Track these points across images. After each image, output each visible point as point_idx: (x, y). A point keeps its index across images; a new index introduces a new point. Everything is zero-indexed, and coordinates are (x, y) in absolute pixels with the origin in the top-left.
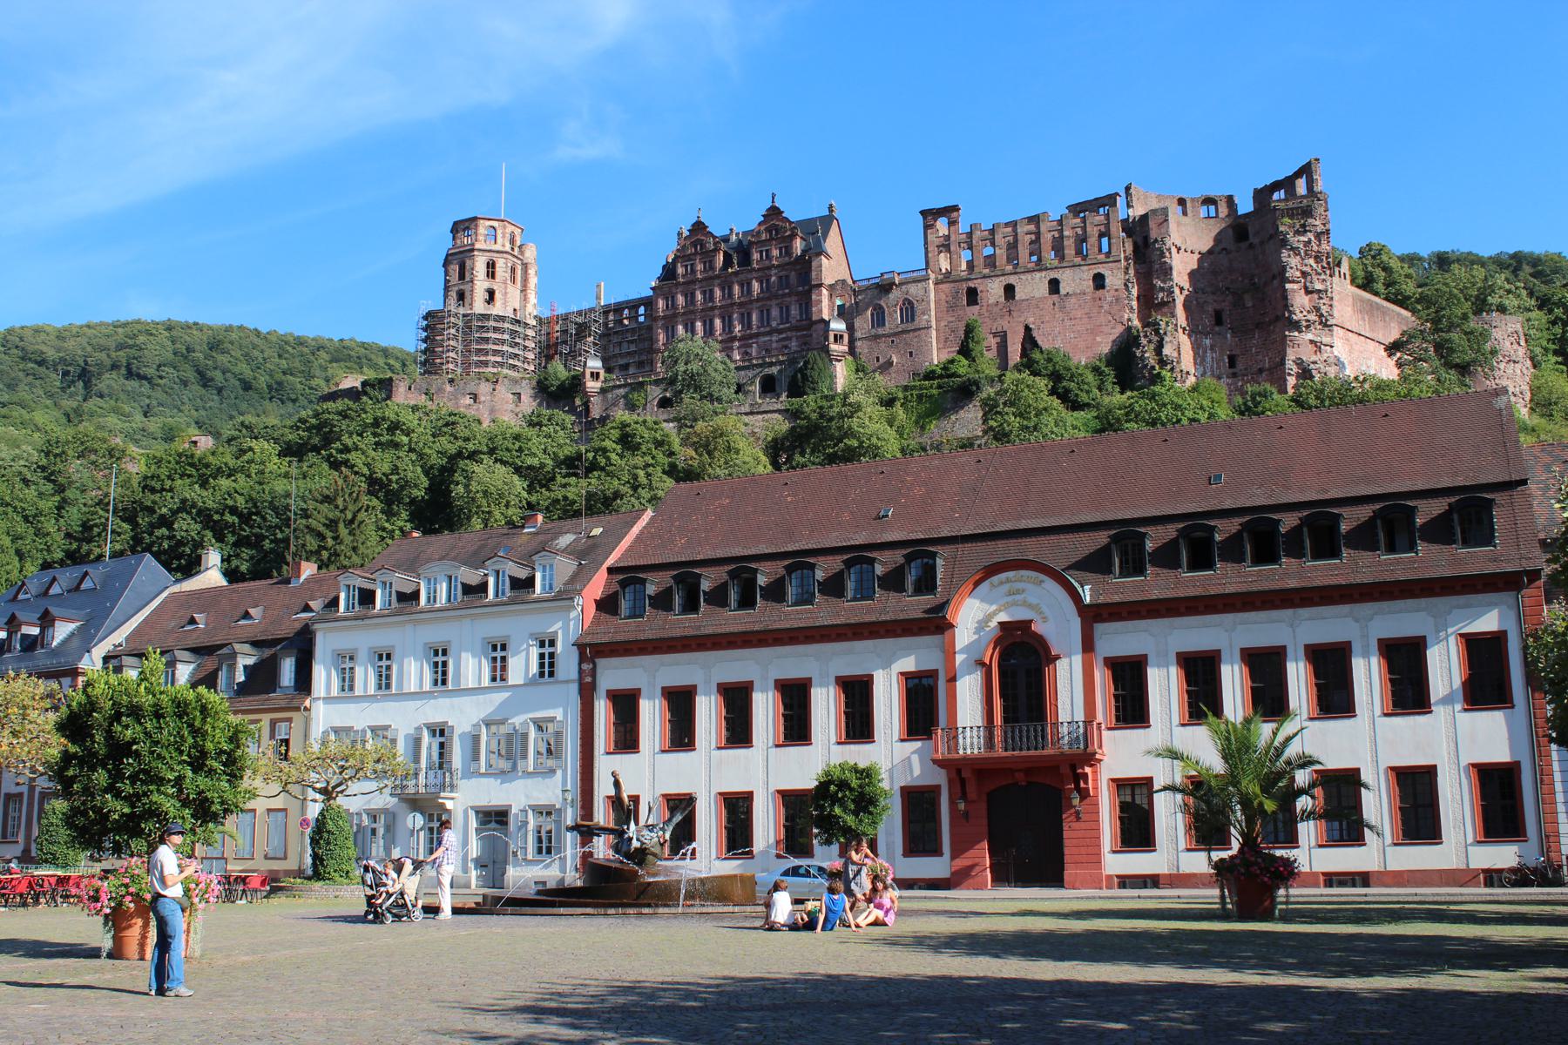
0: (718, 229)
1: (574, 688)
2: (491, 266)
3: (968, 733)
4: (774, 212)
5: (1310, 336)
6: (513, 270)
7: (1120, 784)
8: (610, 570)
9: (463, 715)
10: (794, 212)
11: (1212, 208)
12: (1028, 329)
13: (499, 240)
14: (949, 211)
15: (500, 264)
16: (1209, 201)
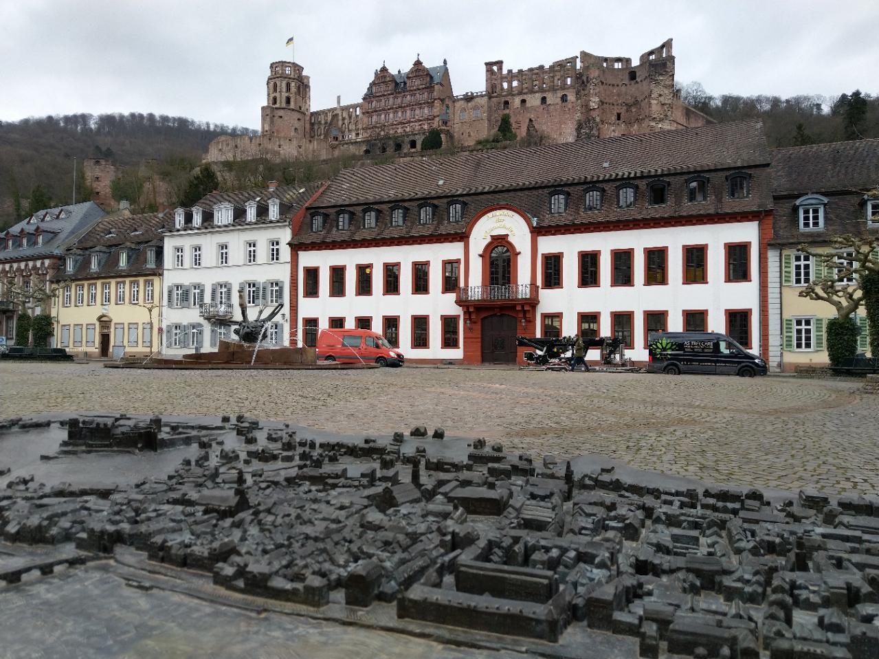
0: (393, 71)
1: (289, 266)
2: (288, 85)
3: (476, 290)
4: (418, 63)
5: (660, 126)
6: (299, 87)
7: (545, 316)
8: (307, 209)
9: (236, 277)
10: (428, 64)
11: (620, 64)
12: (531, 120)
14: (499, 63)
15: (293, 84)
16: (619, 60)
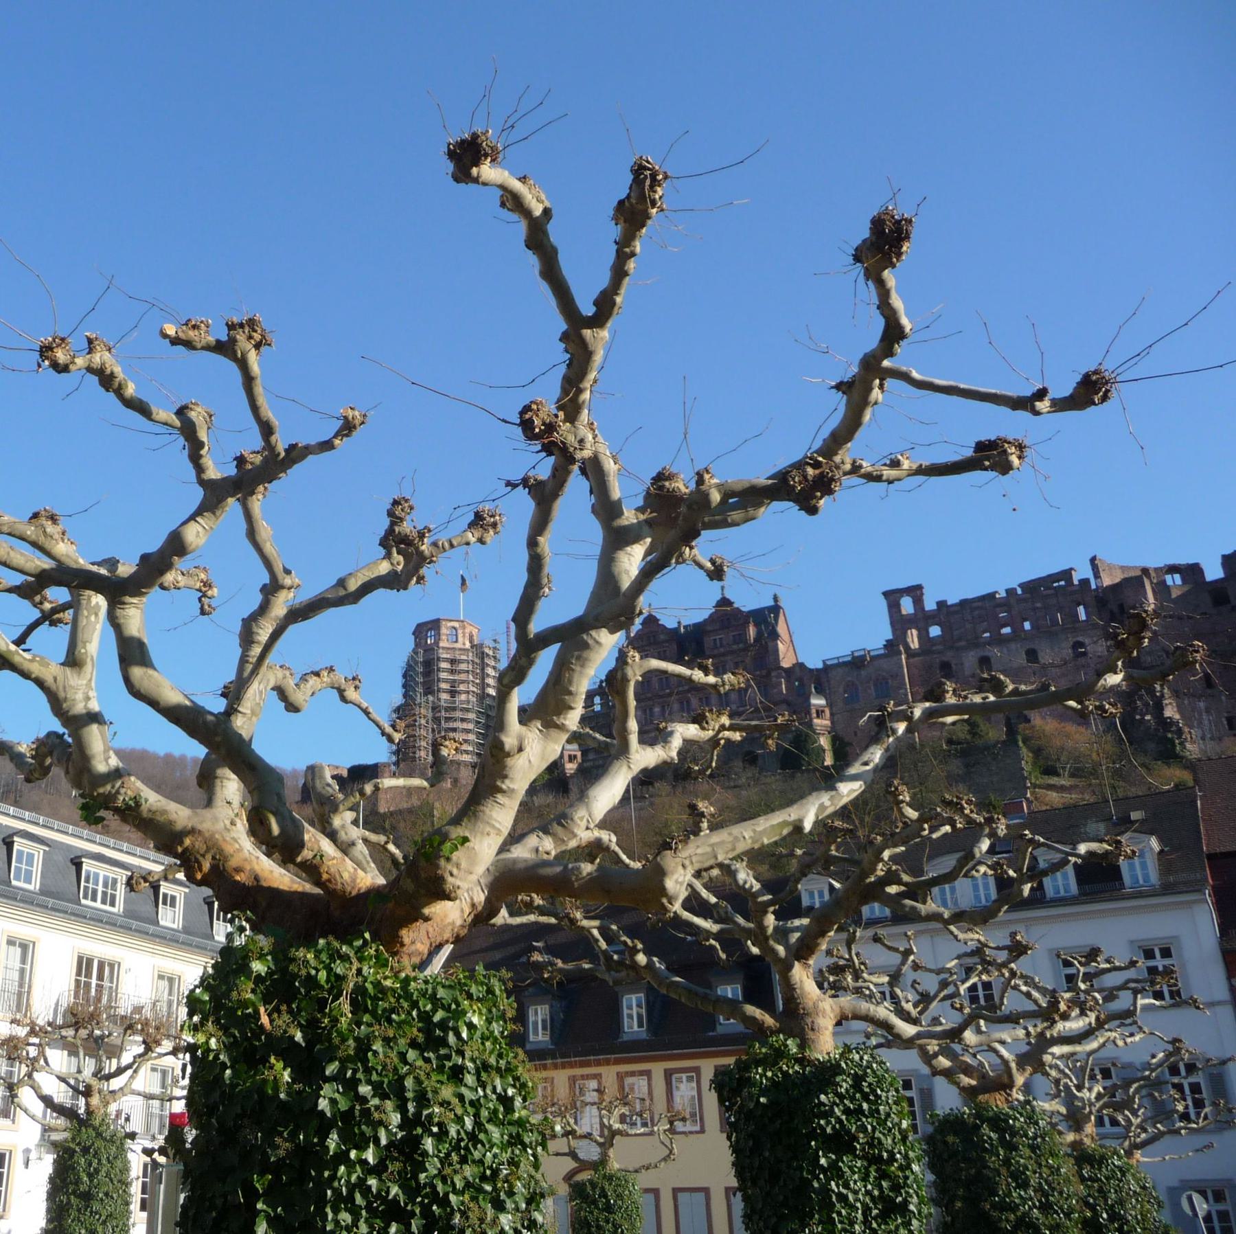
11: (1177, 577)
13: (460, 639)
14: (915, 592)
